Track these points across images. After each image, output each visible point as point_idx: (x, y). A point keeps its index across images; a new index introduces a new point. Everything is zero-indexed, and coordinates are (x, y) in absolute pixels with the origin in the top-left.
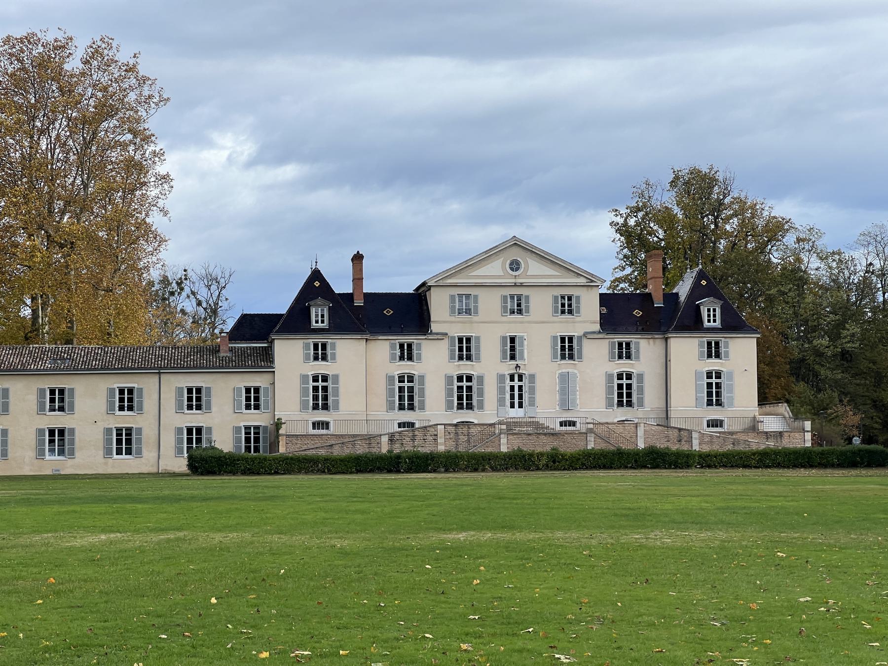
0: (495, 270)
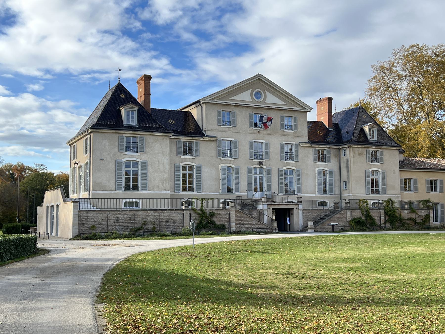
0: (245, 97)
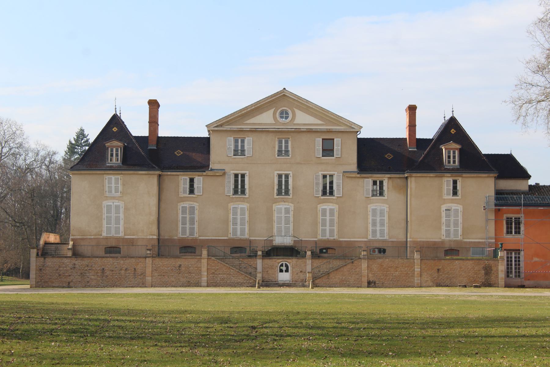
0: (266, 118)
